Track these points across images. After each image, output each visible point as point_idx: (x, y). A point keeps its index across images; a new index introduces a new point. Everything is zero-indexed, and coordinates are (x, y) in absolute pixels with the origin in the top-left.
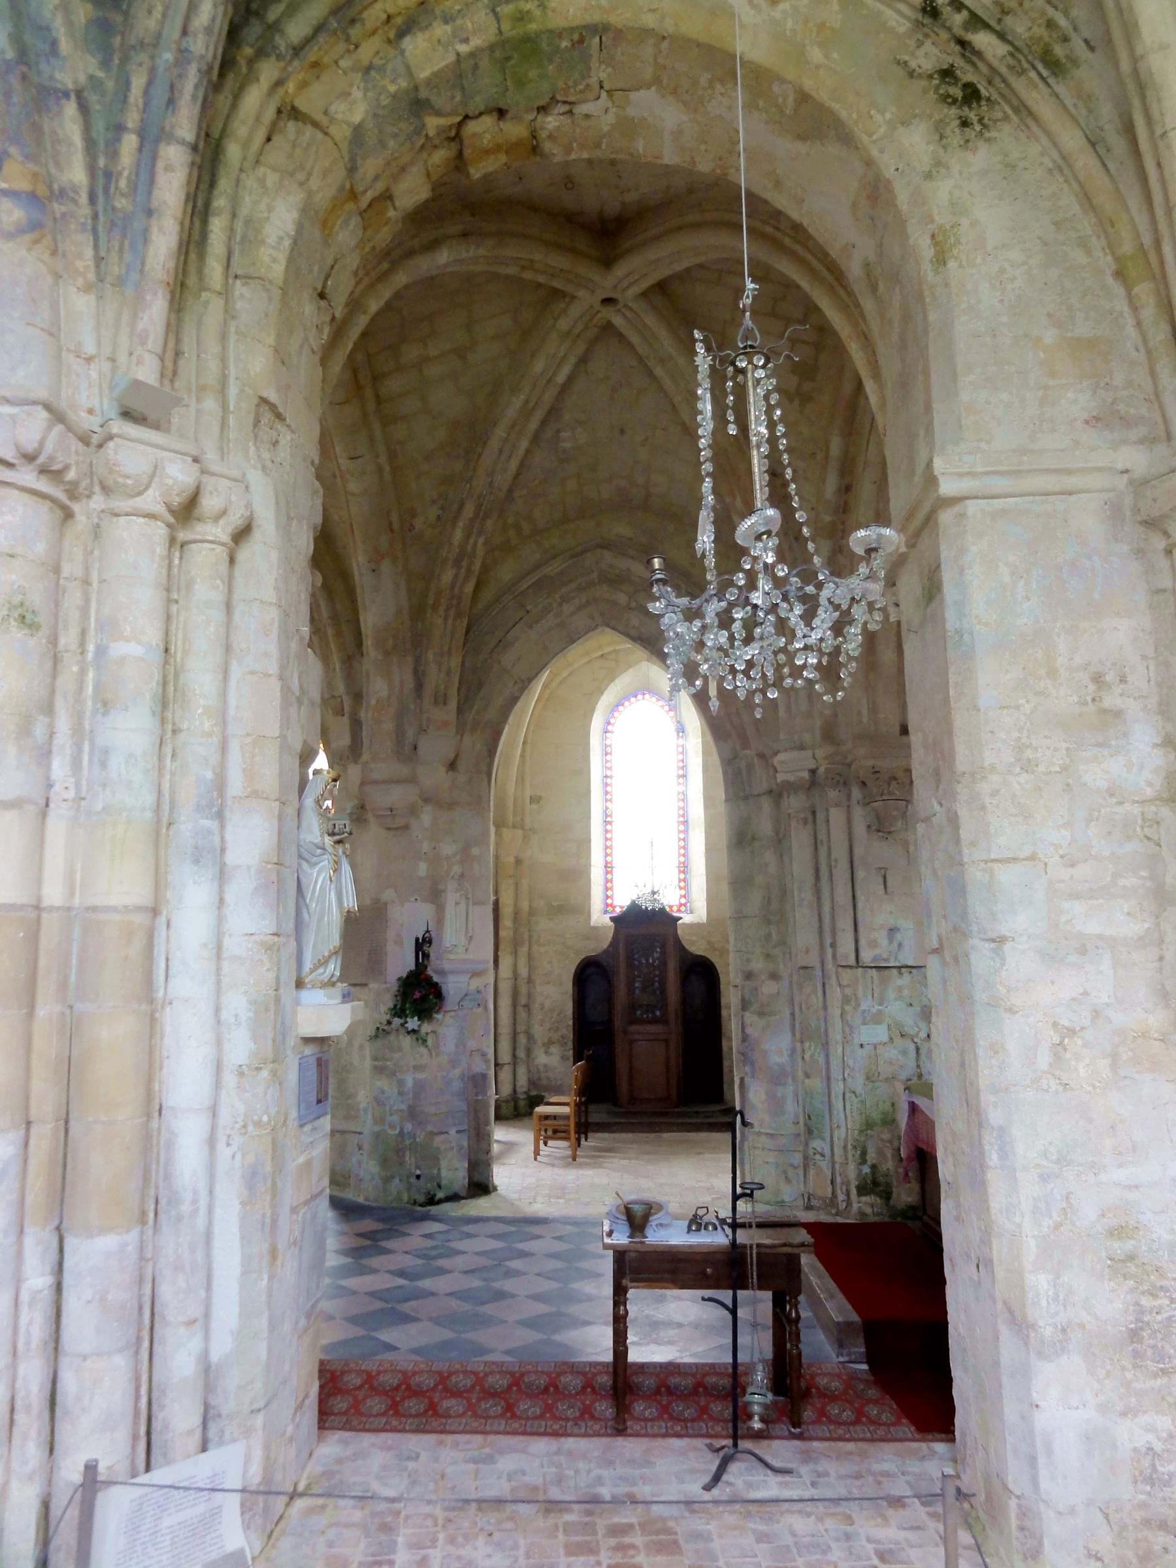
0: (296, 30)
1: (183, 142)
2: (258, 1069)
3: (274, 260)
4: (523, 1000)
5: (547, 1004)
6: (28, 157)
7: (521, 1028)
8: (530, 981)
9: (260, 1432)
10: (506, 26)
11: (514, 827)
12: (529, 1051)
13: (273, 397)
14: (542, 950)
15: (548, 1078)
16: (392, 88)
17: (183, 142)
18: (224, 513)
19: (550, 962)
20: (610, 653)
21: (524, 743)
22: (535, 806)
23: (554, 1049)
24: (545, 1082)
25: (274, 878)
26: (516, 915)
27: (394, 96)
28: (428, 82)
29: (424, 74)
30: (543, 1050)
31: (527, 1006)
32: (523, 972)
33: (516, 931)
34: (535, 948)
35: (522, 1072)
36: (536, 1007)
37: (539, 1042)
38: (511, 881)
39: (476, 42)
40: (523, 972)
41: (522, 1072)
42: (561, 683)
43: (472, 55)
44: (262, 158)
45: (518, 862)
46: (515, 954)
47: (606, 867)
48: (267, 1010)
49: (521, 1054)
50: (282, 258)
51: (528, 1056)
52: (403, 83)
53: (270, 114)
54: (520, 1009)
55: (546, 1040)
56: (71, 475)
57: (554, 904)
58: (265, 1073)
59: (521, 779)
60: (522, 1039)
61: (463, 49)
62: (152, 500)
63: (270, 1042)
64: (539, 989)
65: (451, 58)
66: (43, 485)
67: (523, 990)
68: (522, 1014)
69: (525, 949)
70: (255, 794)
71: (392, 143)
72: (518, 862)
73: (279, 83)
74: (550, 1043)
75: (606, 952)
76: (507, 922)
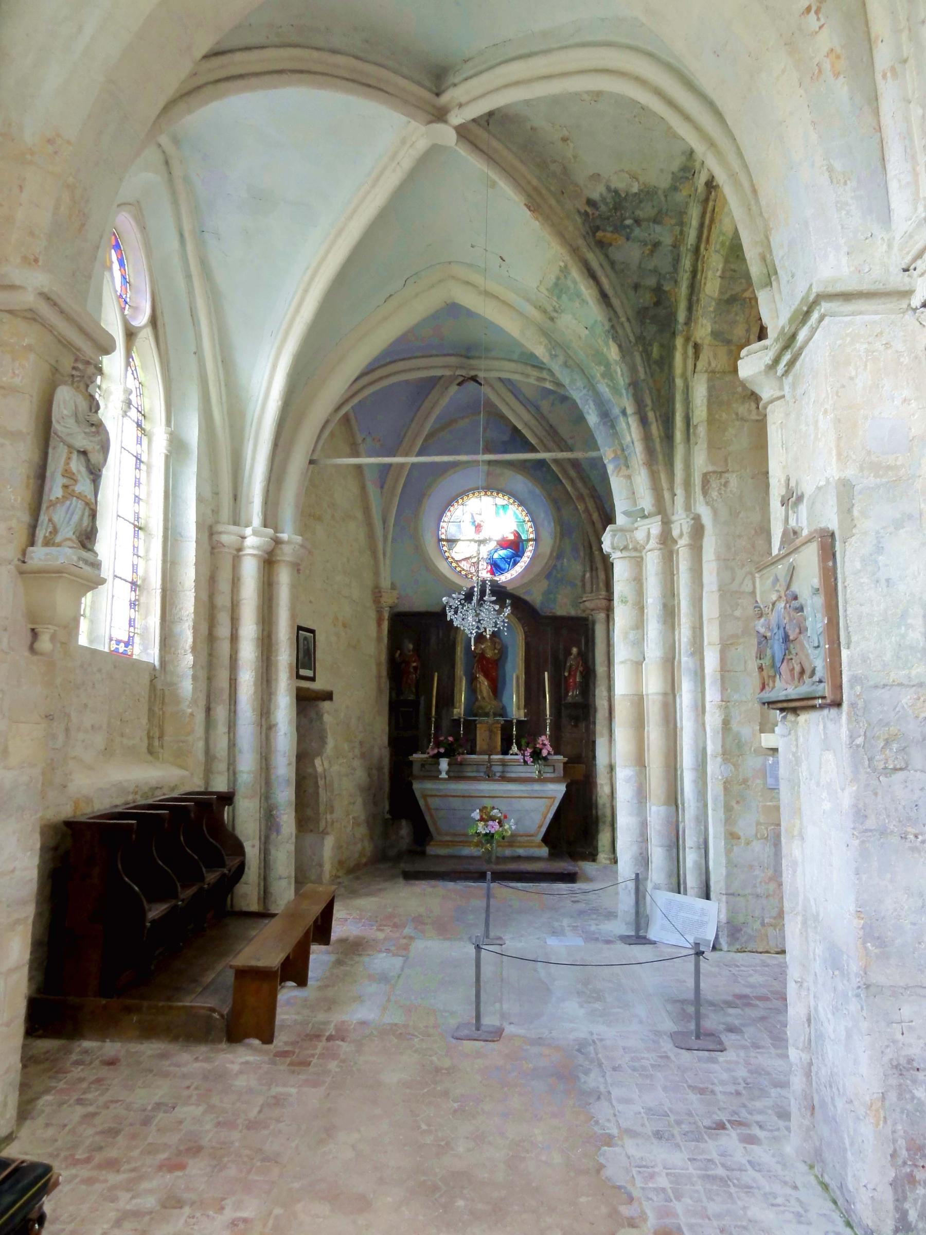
0: (681, 316)
1: (631, 415)
2: (716, 757)
3: (702, 411)
6: (610, 448)
9: (725, 903)
10: (722, 252)
13: (711, 468)
16: (712, 309)
17: (631, 415)
18: (681, 535)
25: (719, 677)
27: (715, 311)
28: (721, 292)
29: (716, 295)
39: (721, 266)
43: (723, 271)
44: (696, 370)
48: (718, 733)
50: (705, 409)
52: (713, 303)
53: (690, 351)
56: (631, 547)
58: (719, 759)
61: (719, 273)
62: (653, 543)
63: (720, 746)
65: (719, 280)
66: (625, 554)
70: (709, 644)
71: (738, 318)
73: (687, 339)
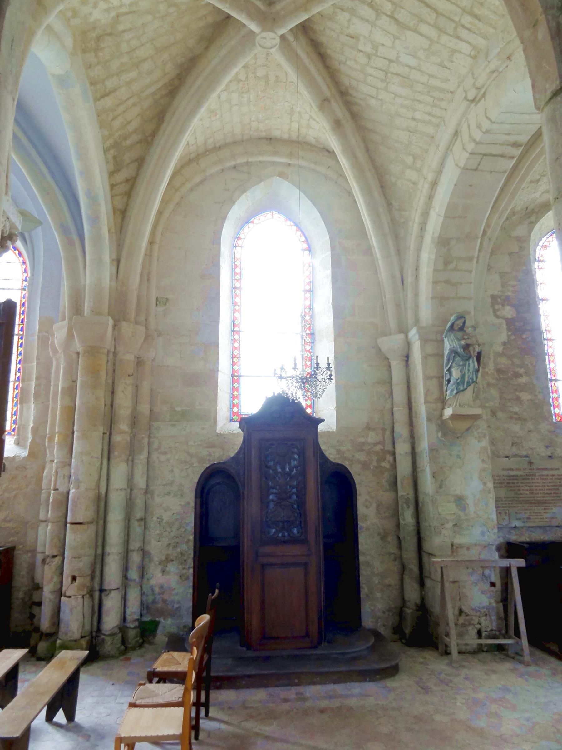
4: (139, 514)
5: (166, 517)
7: (135, 545)
8: (147, 491)
11: (137, 323)
12: (143, 571)
14: (163, 458)
15: (164, 601)
19: (172, 471)
20: (242, 165)
21: (151, 243)
22: (161, 309)
23: (172, 568)
24: (160, 605)
26: (134, 421)
30: (159, 568)
31: (143, 520)
32: (140, 481)
33: (133, 437)
34: (155, 456)
35: (134, 596)
36: (153, 522)
37: (156, 559)
38: (130, 381)
40: (140, 481)
41: (134, 596)
42: (192, 189)
45: (139, 362)
46: (131, 461)
47: (233, 375)
49: (133, 575)
51: (142, 577)
54: (135, 525)
55: (163, 558)
57: (178, 409)
59: (146, 277)
60: (136, 558)
64: (158, 500)
67: (139, 502)
68: (137, 528)
69: (143, 456)
72: (139, 362)
74: (168, 560)
75: (235, 459)
76: (124, 426)
